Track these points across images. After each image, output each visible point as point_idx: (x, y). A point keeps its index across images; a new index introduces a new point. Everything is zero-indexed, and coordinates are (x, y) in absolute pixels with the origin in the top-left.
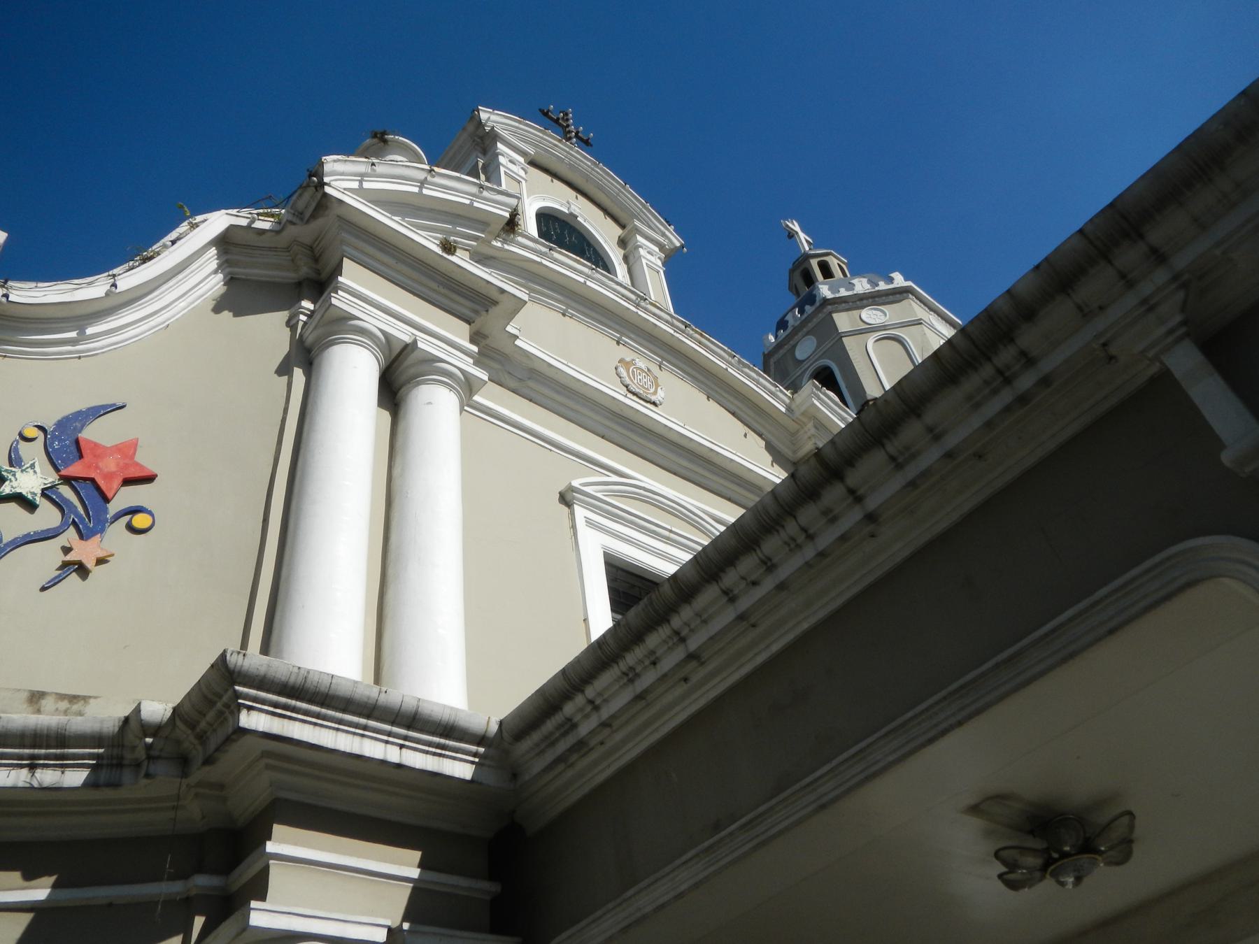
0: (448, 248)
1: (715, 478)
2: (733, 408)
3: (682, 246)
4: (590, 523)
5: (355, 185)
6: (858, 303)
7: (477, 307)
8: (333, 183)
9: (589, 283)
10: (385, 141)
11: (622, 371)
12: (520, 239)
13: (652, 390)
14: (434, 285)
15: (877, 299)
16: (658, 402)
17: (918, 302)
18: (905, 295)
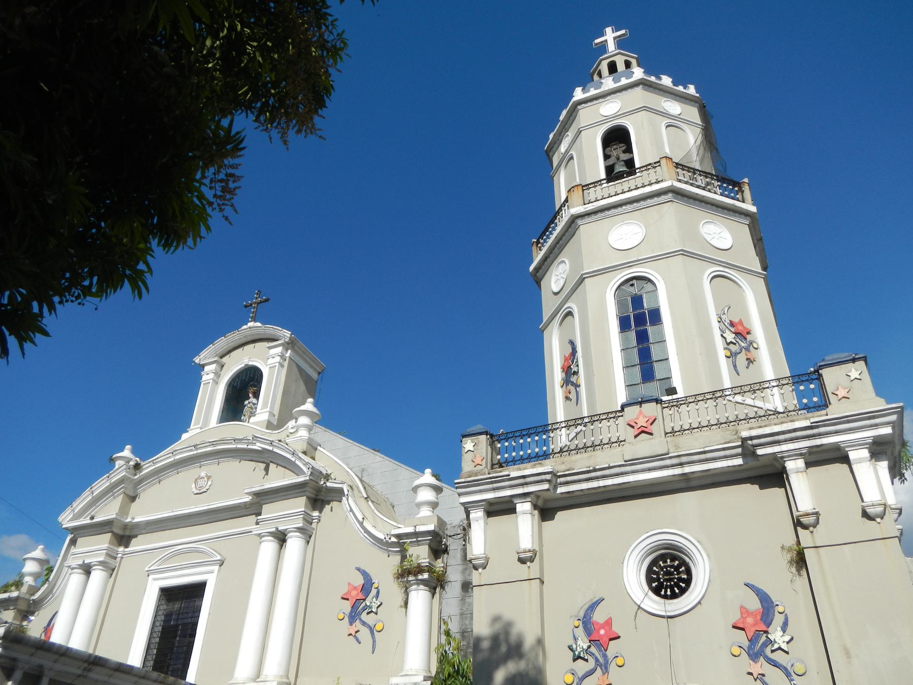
0: (92, 518)
1: (221, 515)
2: (250, 458)
3: (291, 335)
4: (155, 579)
5: (72, 516)
6: (560, 138)
7: (109, 526)
8: (65, 523)
9: (177, 457)
10: (112, 460)
11: (193, 486)
12: (144, 467)
13: (206, 484)
14: (97, 529)
15: (566, 126)
16: (206, 490)
17: (589, 104)
18: (576, 109)
